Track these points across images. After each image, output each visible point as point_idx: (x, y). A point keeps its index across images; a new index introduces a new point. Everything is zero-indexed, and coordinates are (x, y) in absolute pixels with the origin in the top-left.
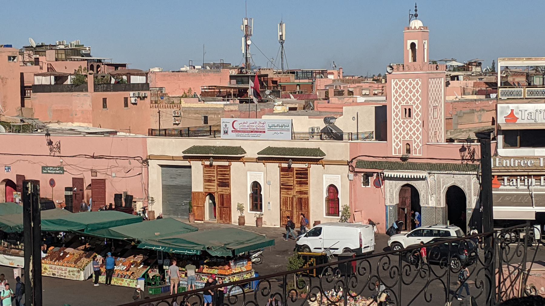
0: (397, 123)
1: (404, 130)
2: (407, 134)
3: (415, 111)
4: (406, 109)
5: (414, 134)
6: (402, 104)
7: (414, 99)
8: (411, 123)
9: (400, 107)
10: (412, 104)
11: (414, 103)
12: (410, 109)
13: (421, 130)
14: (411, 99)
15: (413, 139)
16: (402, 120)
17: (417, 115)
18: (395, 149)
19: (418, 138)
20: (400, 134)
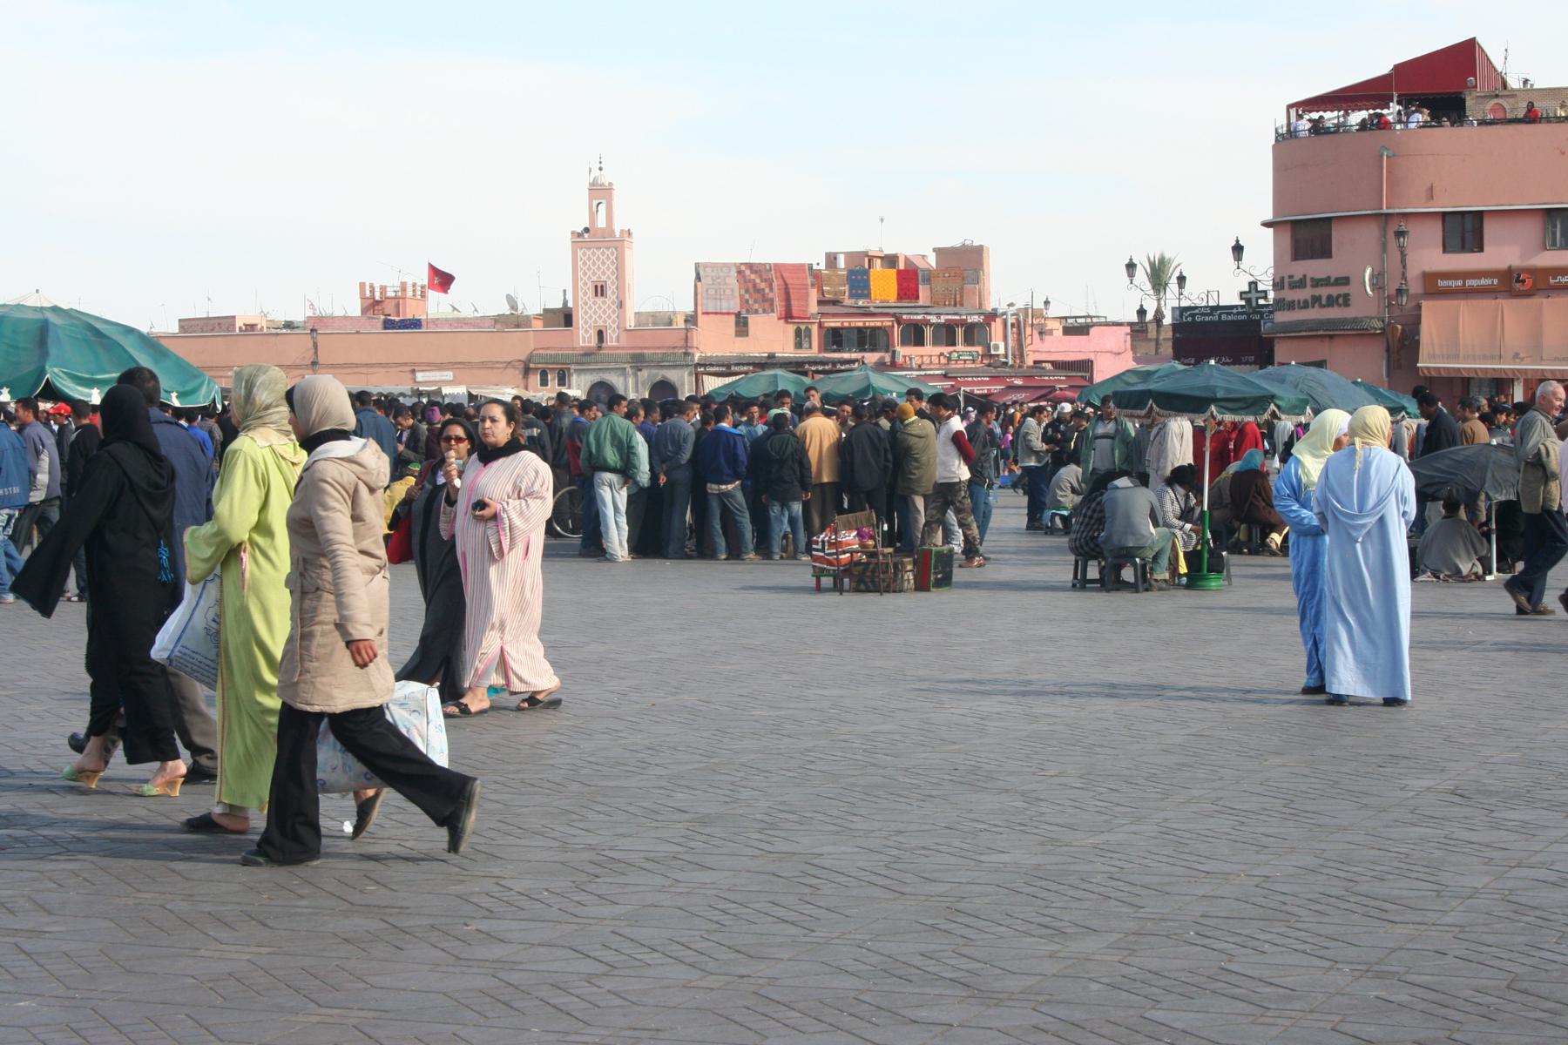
0: (586, 303)
1: (595, 312)
2: (600, 317)
4: (596, 287)
5: (609, 317)
7: (609, 273)
8: (604, 303)
9: (589, 284)
12: (602, 287)
17: (613, 293)
18: (584, 337)
20: (591, 317)
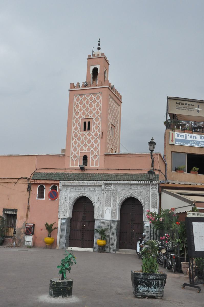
0: (76, 136)
3: (94, 123)
6: (82, 118)
9: (80, 120)
10: (92, 117)
11: (94, 116)
12: (89, 123)
13: (99, 141)
14: (91, 113)
15: (91, 151)
16: (81, 133)
17: (97, 127)
19: (96, 149)
